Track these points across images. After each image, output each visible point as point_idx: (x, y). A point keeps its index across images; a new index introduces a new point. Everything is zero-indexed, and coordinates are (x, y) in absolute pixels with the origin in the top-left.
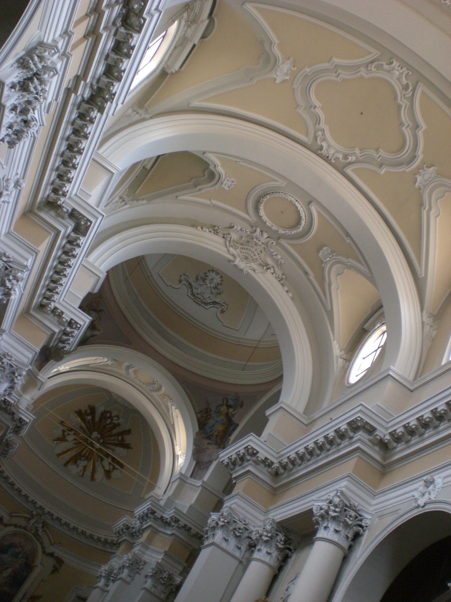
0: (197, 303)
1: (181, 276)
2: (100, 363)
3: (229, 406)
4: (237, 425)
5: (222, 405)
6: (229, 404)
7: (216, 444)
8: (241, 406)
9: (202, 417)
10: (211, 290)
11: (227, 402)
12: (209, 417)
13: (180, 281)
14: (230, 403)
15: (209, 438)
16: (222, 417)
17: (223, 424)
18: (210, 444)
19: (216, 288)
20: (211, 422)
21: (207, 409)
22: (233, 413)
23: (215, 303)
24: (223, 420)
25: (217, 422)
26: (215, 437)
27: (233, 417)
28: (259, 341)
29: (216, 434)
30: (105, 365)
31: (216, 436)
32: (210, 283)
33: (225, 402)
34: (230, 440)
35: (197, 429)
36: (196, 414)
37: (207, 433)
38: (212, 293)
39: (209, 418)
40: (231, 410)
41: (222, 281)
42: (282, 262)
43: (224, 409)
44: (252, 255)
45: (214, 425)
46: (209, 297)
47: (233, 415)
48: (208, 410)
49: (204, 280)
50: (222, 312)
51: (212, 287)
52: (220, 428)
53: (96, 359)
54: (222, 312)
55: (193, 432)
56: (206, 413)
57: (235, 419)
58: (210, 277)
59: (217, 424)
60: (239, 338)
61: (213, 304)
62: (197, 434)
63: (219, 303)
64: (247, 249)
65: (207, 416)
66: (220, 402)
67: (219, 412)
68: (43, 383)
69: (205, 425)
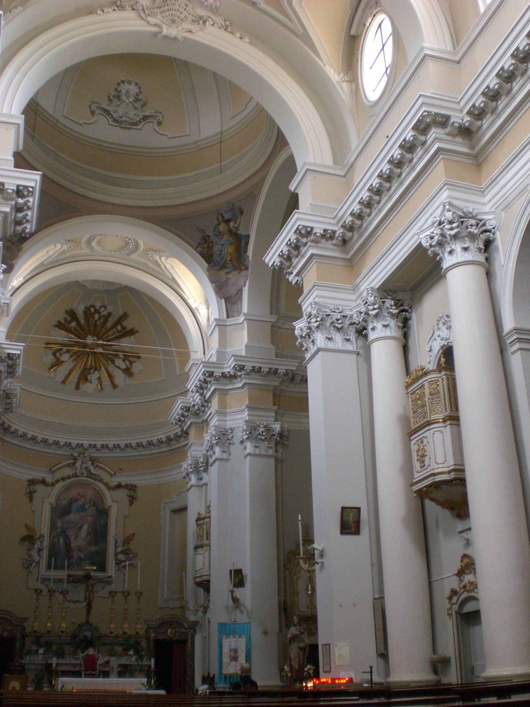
0: (126, 128)
1: (90, 107)
2: (54, 254)
3: (227, 222)
4: (248, 237)
5: (219, 224)
6: (226, 218)
7: (235, 269)
8: (242, 213)
9: (203, 249)
10: (133, 106)
11: (223, 217)
12: (211, 244)
13: (93, 113)
14: (227, 216)
15: (223, 267)
16: (226, 237)
17: (232, 244)
18: (228, 272)
19: (137, 100)
20: (216, 249)
21: (204, 238)
22: (236, 226)
23: (145, 119)
24: (229, 240)
25: (223, 245)
26: (230, 262)
27: (239, 230)
28: (221, 133)
29: (229, 258)
30: (61, 254)
31: (230, 260)
32: (128, 98)
33: (220, 219)
34: (248, 257)
35: (206, 265)
36: (195, 249)
37: (219, 264)
38: (136, 108)
39: (212, 246)
40: (232, 224)
41: (140, 88)
42: (217, 6)
43: (223, 227)
44: (178, 14)
45: (222, 251)
46: (135, 115)
47: (237, 228)
48: (207, 238)
49: (119, 97)
50: (159, 123)
51: (131, 101)
52: (230, 250)
53: (47, 252)
54: (159, 123)
55: (203, 269)
56: (206, 242)
57: (242, 231)
58: (124, 91)
59: (225, 248)
60: (196, 142)
61: (144, 120)
62: (208, 270)
63: (150, 116)
64: (168, 10)
65: (209, 245)
66: (216, 222)
67: (220, 233)
68: (8, 304)
69: (211, 255)
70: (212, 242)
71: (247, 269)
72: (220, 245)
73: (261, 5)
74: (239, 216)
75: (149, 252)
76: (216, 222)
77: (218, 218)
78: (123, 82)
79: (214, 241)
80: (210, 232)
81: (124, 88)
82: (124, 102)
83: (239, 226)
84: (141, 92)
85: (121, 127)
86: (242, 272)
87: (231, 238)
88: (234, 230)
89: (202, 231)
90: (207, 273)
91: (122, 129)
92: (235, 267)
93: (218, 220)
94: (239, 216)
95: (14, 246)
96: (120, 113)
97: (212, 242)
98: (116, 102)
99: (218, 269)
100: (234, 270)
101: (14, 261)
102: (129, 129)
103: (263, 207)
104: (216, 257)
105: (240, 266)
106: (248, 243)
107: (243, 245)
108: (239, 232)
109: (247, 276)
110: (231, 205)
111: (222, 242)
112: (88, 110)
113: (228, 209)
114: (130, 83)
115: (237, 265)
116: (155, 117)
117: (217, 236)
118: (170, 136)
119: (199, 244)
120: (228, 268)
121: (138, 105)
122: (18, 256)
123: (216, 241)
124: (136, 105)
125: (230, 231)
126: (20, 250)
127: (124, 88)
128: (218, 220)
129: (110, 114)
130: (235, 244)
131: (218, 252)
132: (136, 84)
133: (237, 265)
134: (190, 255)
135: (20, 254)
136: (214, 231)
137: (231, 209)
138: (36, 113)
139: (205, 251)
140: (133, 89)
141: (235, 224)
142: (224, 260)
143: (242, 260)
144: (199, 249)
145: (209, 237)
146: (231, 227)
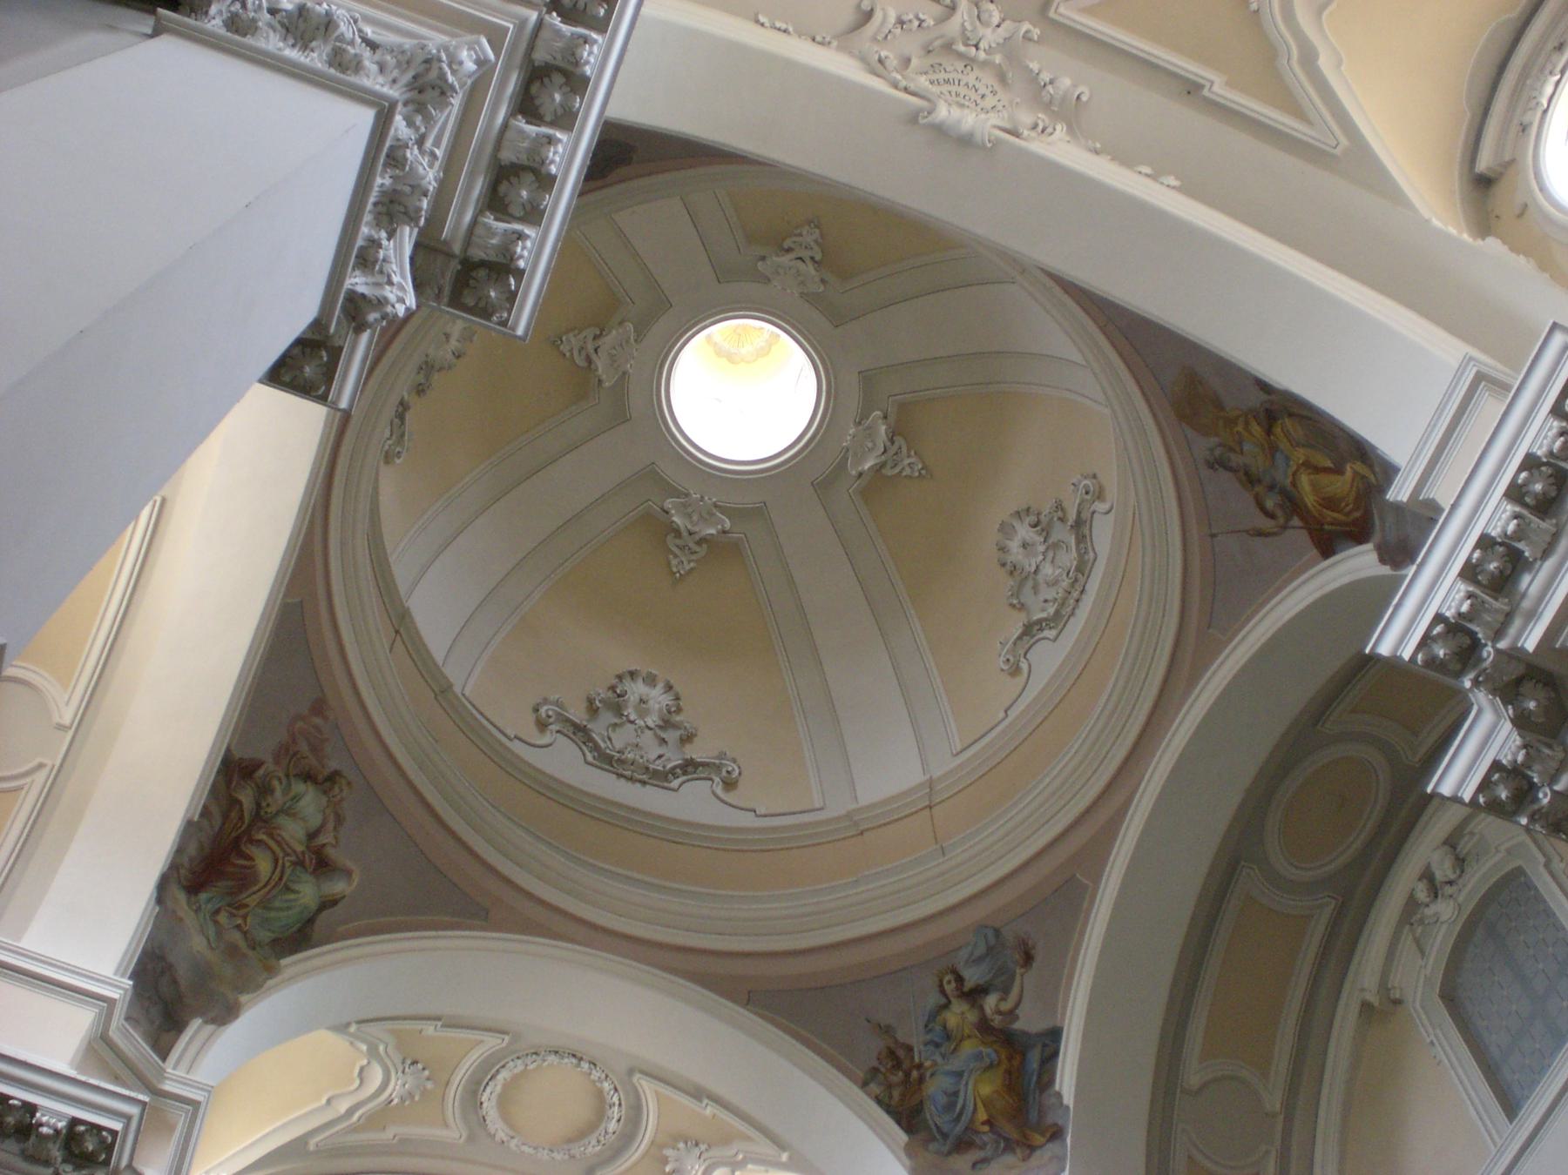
0: (630, 779)
1: (536, 710)
2: (351, 1112)
3: (974, 995)
4: (1055, 1035)
5: (947, 1006)
6: (969, 985)
7: (1009, 1147)
8: (1028, 959)
9: (890, 1087)
10: (656, 736)
11: (959, 979)
12: (915, 1074)
13: (542, 726)
14: (973, 977)
15: (962, 1145)
16: (968, 1047)
17: (991, 1066)
18: (985, 1161)
19: (666, 724)
20: (936, 1087)
21: (892, 1053)
22: (1005, 1006)
23: (690, 769)
24: (979, 1057)
25: (959, 1075)
26: (986, 1128)
27: (1017, 1018)
28: (931, 783)
29: (982, 1115)
30: (376, 1120)
31: (988, 1122)
32: (643, 714)
33: (950, 988)
34: (1059, 1095)
35: (903, 1137)
36: (864, 1085)
37: (945, 1136)
38: (663, 741)
39: (921, 1080)
40: (990, 1002)
41: (677, 698)
42: (1084, 98)
43: (959, 1015)
44: (974, 96)
45: (956, 1094)
46: (660, 757)
47: (1012, 1014)
48: (901, 1053)
49: (618, 709)
50: (729, 785)
51: (651, 724)
52: (986, 1090)
53: (329, 1101)
54: (729, 785)
55: (893, 1152)
56: (898, 1065)
57: (1029, 1021)
58: (632, 698)
59: (966, 1082)
60: (849, 815)
61: (685, 773)
62: (910, 1151)
63: (704, 765)
64: (947, 82)
65: (908, 1074)
66: (934, 999)
67: (948, 1036)
68: (195, 1104)
69: (918, 1110)
70: (920, 1066)
71: (1057, 1134)
72: (949, 1073)
73: (1216, 88)
74: (1019, 971)
75: (669, 1152)
76: (934, 999)
77: (941, 986)
78: (633, 674)
79: (928, 1064)
80: (913, 1034)
81: (636, 689)
82: (632, 722)
83: (1017, 1005)
84: (679, 710)
85: (620, 776)
86: (1038, 1153)
87: (986, 1050)
88: (997, 1021)
89: (887, 1030)
90: (907, 1162)
91: (623, 780)
92: (1006, 1140)
93: (943, 992)
94: (1019, 971)
95: (250, 953)
96: (618, 745)
97: (920, 1066)
98: (607, 717)
99: (946, 1149)
100: (1005, 1149)
101: (243, 998)
102: (644, 783)
103: (1117, 906)
104: (932, 1114)
105: (1025, 1136)
106: (1055, 1054)
107: (1035, 1065)
108: (1018, 1026)
109: (1061, 1159)
110: (990, 934)
111: (956, 1064)
112: (531, 718)
113: (981, 949)
114: (651, 680)
115: (1015, 1135)
116: (718, 768)
117: (937, 1045)
118: (762, 810)
119: (875, 1071)
120: (982, 1147)
121: (672, 736)
122: (259, 986)
123: (935, 1063)
124: (663, 735)
125: (984, 1026)
126: (271, 971)
127: (636, 689)
128: (943, 992)
129: (591, 740)
130: (1004, 1066)
131: (942, 1100)
132: (669, 688)
133: (1015, 1135)
134: (848, 1105)
135: (271, 982)
136: (927, 1028)
137: (990, 949)
138: (397, 632)
139: (896, 1093)
140: (658, 699)
141: (1003, 999)
142: (965, 1119)
143: (1033, 1115)
144: (875, 1088)
145: (910, 1049)
146: (988, 1010)
